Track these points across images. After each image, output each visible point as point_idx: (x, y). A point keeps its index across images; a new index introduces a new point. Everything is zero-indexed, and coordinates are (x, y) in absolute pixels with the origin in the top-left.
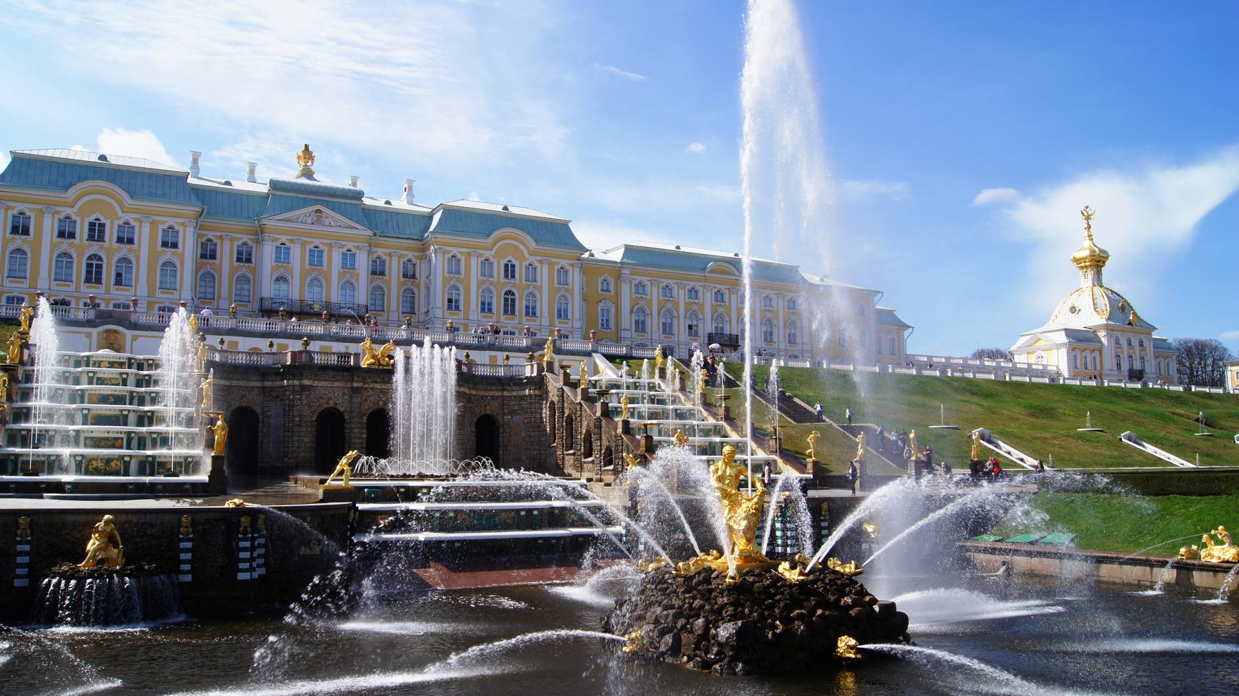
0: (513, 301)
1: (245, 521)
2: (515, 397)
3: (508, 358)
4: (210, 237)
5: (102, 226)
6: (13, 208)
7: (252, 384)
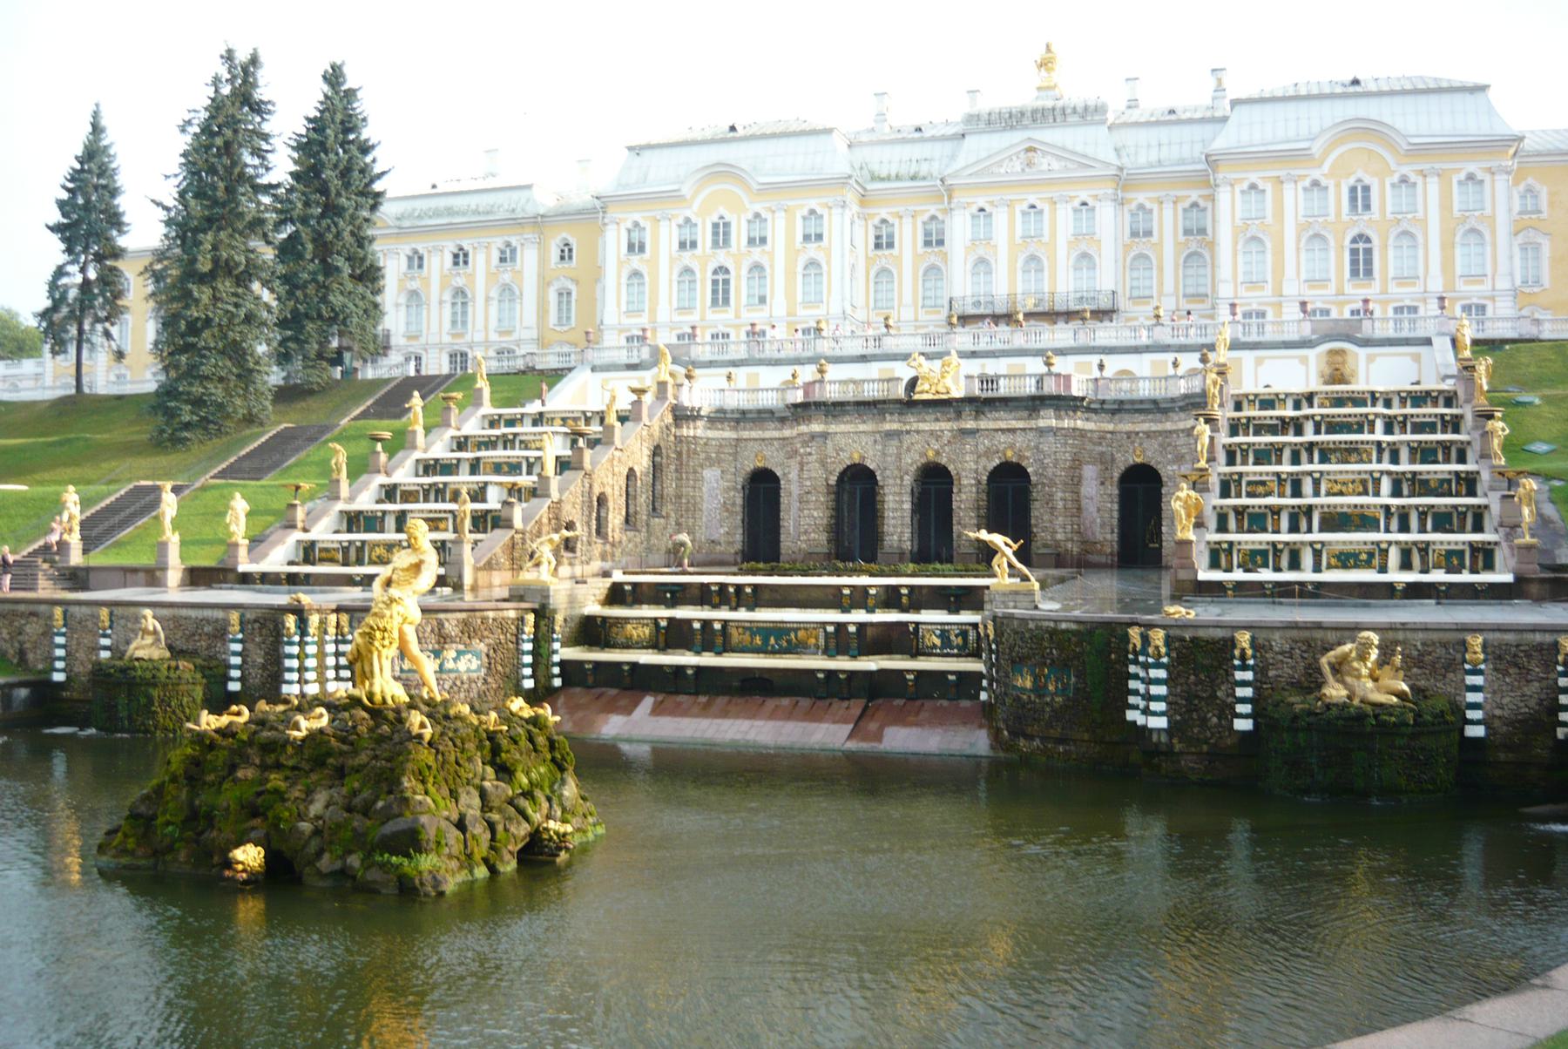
0: (1368, 252)
1: (291, 621)
2: (1183, 431)
3: (1175, 364)
4: (885, 216)
5: (726, 225)
6: (625, 220)
7: (768, 434)
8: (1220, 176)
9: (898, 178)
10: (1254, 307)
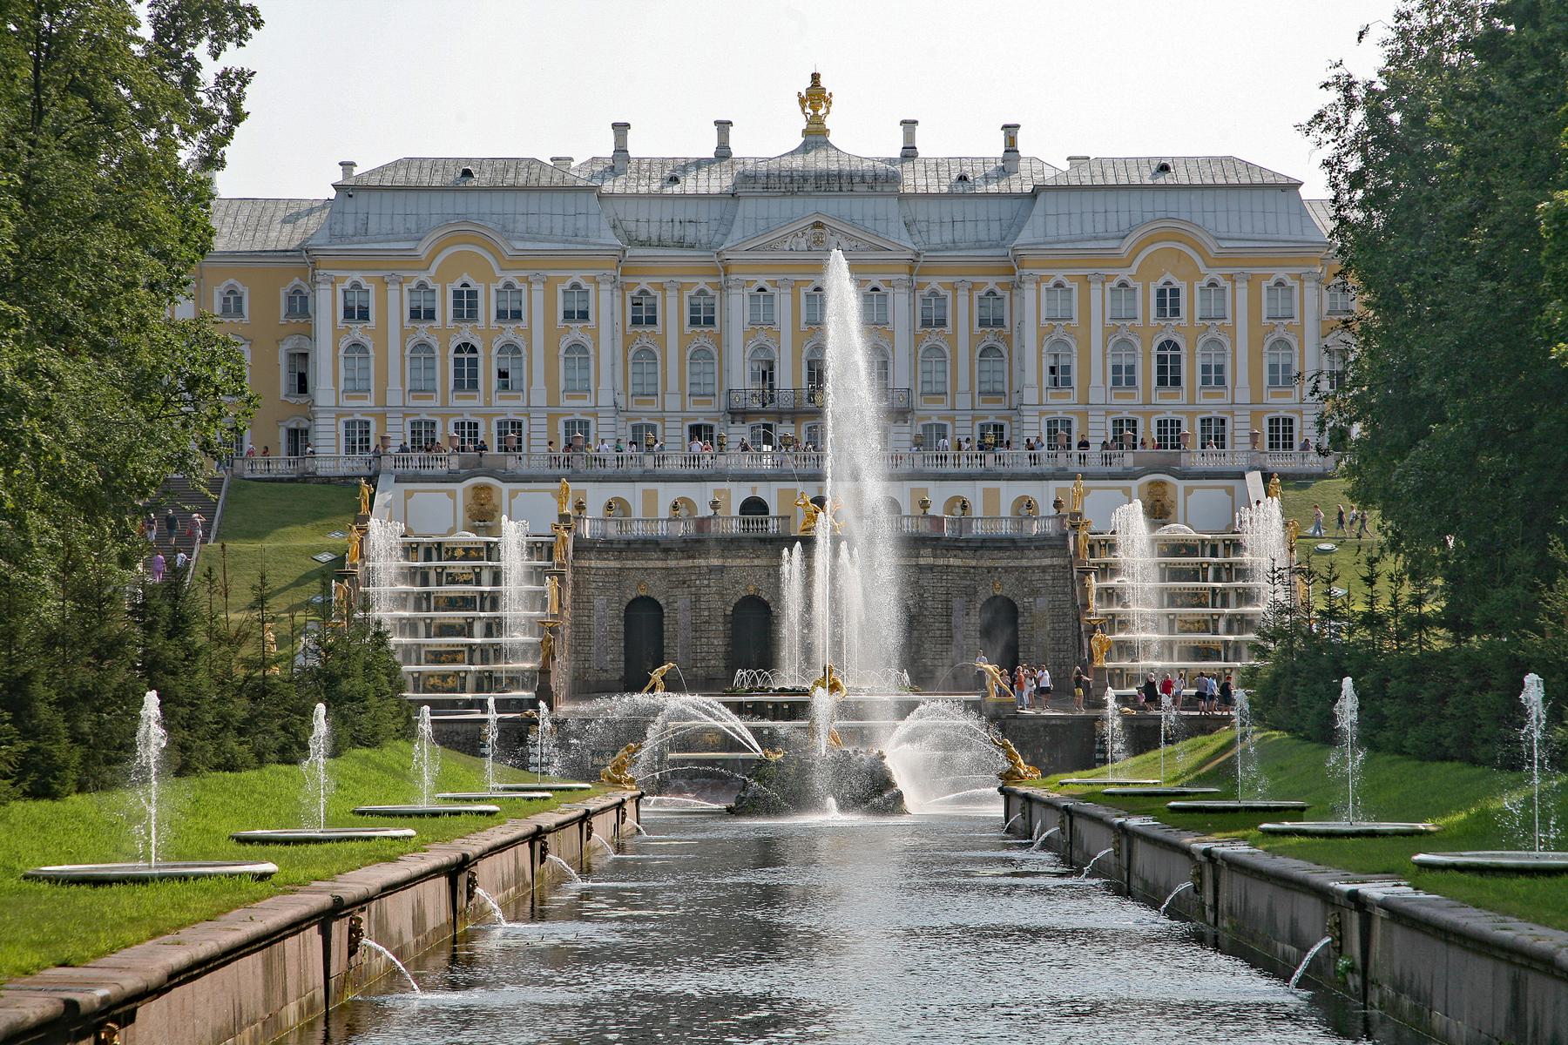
0: (1177, 359)
2: (1038, 567)
4: (644, 286)
5: (473, 294)
8: (1027, 271)
9: (661, 244)
10: (1060, 414)
